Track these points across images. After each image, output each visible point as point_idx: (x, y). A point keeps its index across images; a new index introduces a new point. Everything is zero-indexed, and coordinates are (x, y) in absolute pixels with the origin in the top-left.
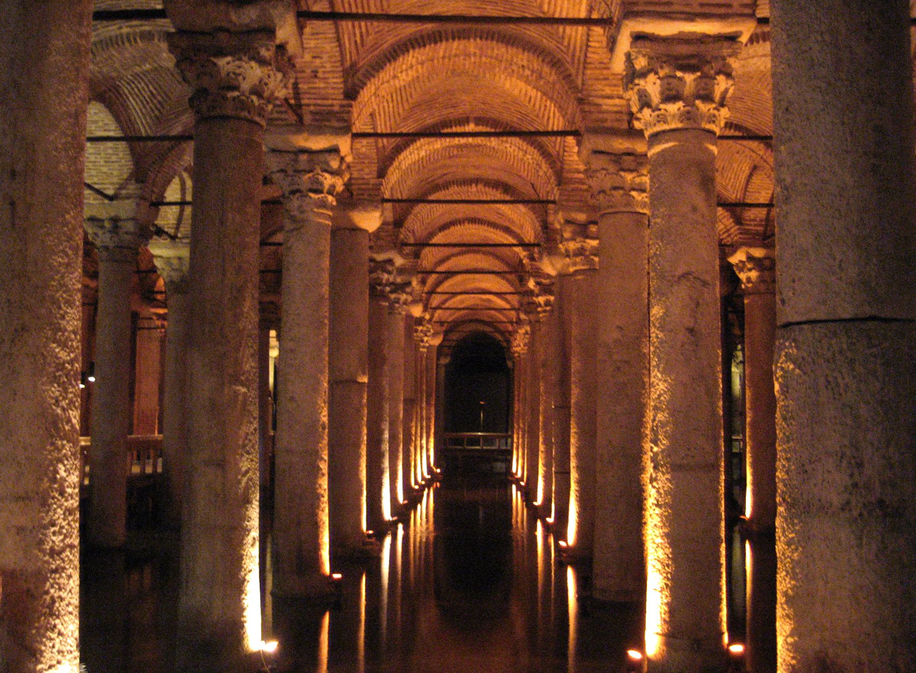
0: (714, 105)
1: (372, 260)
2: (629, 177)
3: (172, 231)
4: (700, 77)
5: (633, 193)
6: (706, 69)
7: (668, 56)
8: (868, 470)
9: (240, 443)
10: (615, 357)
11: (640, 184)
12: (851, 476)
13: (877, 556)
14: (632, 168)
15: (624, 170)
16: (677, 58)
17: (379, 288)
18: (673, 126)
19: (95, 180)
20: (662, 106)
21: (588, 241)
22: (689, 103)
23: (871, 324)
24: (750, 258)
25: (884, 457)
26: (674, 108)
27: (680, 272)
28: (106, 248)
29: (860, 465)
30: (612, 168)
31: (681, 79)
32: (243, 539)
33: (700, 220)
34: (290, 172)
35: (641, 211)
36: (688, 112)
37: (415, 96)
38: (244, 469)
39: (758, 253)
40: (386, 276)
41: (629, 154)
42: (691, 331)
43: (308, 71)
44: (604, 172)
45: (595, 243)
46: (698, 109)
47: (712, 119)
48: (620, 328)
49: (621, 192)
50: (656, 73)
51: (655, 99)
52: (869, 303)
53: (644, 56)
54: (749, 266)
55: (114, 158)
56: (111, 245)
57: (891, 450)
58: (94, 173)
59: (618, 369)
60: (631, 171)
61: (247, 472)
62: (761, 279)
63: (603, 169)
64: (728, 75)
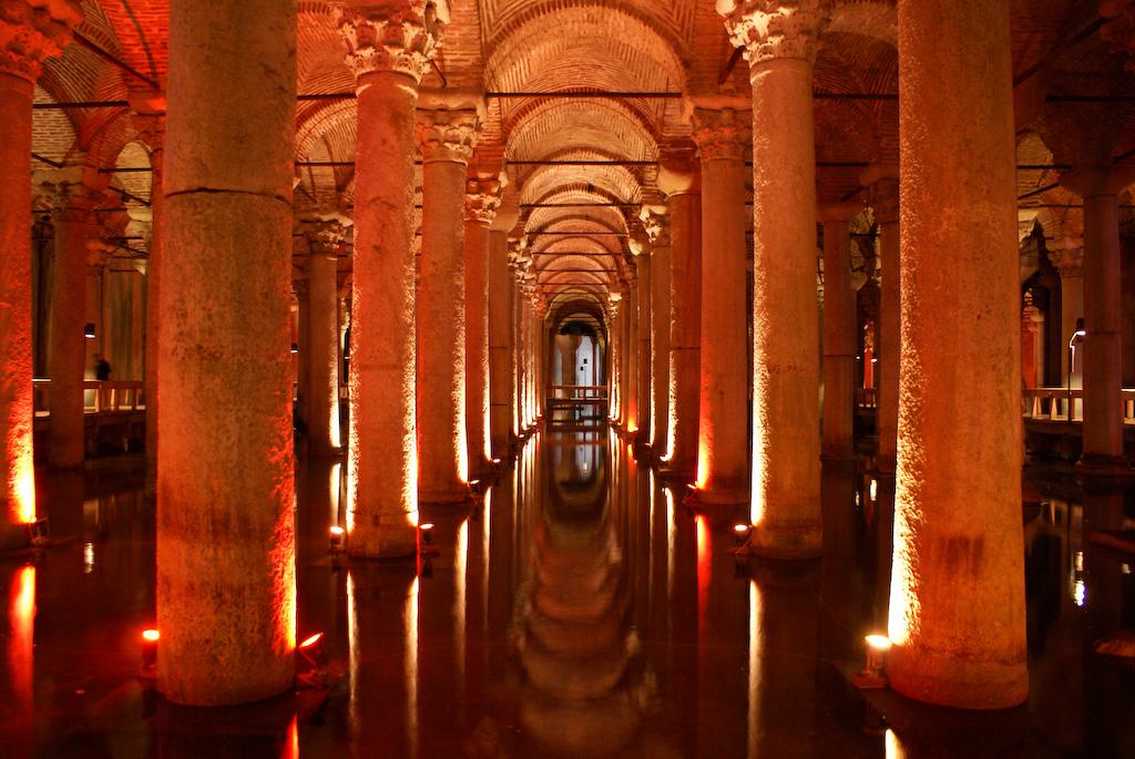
0: (402, 50)
1: (319, 221)
2: (443, 130)
3: (147, 199)
4: (389, 25)
5: (447, 145)
6: (393, 18)
7: (361, 7)
8: (191, 321)
9: (4, 350)
10: (430, 289)
11: (454, 136)
12: (179, 325)
13: (195, 393)
14: (445, 122)
16: (369, 9)
17: (326, 245)
18: (368, 70)
19: (45, 149)
20: (358, 53)
22: (378, 48)
23: (198, 195)
24: (653, 215)
25: (204, 309)
26: (368, 53)
27: (371, 196)
28: (59, 209)
29: (185, 315)
30: (428, 123)
31: (372, 27)
32: (7, 430)
33: (389, 151)
34: (153, 132)
36: (380, 57)
37: (308, 70)
38: (8, 372)
39: (660, 210)
40: (332, 235)
43: (158, 42)
46: (388, 53)
47: (405, 63)
48: (434, 263)
49: (436, 144)
50: (351, 23)
51: (355, 46)
52: (199, 177)
53: (339, 8)
54: (652, 222)
55: (58, 130)
56: (63, 206)
57: (210, 301)
58: (43, 143)
59: (432, 299)
60: (444, 125)
61: (12, 374)
62: (664, 235)
64: (414, 23)
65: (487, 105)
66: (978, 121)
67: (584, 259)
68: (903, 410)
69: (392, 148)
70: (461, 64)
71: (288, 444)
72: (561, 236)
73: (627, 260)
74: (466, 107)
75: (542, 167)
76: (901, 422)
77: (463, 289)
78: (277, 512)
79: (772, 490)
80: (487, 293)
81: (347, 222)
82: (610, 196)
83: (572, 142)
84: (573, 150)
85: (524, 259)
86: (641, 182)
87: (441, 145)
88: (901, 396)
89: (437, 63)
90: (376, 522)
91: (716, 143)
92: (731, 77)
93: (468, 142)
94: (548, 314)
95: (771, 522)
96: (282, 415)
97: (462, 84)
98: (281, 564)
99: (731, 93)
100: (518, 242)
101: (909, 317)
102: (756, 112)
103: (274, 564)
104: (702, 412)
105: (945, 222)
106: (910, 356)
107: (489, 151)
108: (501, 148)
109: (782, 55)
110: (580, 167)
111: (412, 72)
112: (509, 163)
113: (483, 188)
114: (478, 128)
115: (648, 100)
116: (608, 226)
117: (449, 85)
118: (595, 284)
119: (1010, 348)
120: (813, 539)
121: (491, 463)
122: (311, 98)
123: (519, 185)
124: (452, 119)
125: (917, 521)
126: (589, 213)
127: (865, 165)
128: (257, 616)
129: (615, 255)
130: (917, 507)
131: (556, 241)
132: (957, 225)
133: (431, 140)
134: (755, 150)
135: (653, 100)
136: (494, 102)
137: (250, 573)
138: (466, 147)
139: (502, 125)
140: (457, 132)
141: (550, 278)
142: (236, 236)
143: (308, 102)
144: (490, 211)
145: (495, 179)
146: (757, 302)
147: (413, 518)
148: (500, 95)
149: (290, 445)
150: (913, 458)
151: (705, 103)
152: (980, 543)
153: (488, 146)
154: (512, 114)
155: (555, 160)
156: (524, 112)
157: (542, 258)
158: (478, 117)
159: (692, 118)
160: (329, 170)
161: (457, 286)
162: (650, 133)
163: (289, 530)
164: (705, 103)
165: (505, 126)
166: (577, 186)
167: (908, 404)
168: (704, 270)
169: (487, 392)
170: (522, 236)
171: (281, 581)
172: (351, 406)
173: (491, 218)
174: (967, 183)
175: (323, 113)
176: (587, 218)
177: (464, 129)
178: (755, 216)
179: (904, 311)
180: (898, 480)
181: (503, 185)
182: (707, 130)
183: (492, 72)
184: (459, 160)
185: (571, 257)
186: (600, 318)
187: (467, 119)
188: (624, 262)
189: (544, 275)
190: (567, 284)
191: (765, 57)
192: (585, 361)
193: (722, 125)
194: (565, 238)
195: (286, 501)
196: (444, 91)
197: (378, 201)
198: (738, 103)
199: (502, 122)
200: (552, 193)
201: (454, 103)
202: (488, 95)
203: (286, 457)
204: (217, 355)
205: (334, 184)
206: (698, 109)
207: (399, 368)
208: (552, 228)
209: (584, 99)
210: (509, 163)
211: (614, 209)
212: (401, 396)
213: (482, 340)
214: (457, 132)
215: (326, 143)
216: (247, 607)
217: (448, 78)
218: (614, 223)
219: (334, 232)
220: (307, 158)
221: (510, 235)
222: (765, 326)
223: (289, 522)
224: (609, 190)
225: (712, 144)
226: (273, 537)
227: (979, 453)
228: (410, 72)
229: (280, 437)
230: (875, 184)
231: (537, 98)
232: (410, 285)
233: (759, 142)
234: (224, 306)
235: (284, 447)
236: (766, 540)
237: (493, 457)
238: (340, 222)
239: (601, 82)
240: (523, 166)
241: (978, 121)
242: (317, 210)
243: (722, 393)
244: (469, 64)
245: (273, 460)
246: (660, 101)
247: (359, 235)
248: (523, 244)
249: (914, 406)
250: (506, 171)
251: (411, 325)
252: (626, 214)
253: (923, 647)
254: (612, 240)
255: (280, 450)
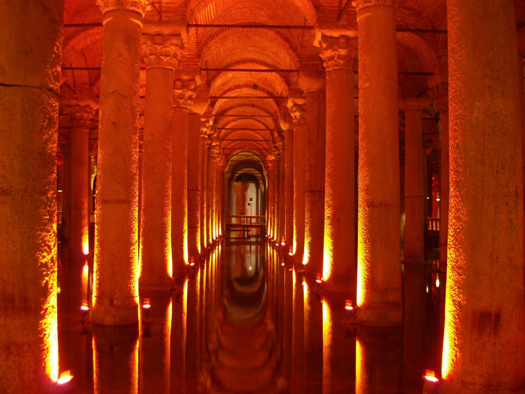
1: (78, 105)
2: (159, 48)
5: (162, 57)
11: (166, 52)
15: (155, 44)
18: (111, 9)
21: (175, 90)
24: (295, 105)
35: (167, 67)
39: (300, 102)
40: (86, 115)
41: (159, 35)
42: (114, 124)
44: (145, 46)
45: (179, 92)
48: (153, 134)
49: (155, 56)
54: (294, 109)
60: (160, 44)
62: (302, 117)
63: (144, 43)
65: (188, 32)
66: (495, 49)
67: (251, 132)
68: (451, 232)
69: (125, 59)
70: (171, 5)
71: (53, 251)
72: (236, 118)
73: (278, 134)
74: (176, 33)
75: (224, 72)
76: (450, 239)
77: (171, 152)
78: (45, 292)
79: (370, 284)
80: (186, 154)
81: (95, 107)
82: (267, 92)
83: (244, 57)
84: (245, 61)
85: (212, 132)
86: (288, 83)
87: (158, 57)
88: (450, 222)
89: (156, 5)
90: (111, 303)
91: (336, 59)
92: (345, 17)
93: (175, 56)
94: (227, 168)
95: (369, 304)
96: (50, 232)
97: (172, 18)
98: (47, 329)
99: (345, 27)
100: (208, 121)
101: (455, 171)
102: (360, 40)
103: (44, 329)
104: (325, 233)
105: (476, 112)
106: (455, 196)
107: (189, 62)
108: (197, 60)
109: (377, 4)
110: (249, 73)
111: (140, 11)
112: (202, 69)
113: (184, 86)
114: (182, 47)
115: (292, 30)
116: (267, 111)
117: (164, 19)
118: (258, 149)
119: (516, 192)
120: (395, 316)
121: (189, 266)
122: (75, 25)
123: (208, 84)
124: (166, 40)
125: (460, 302)
126: (254, 103)
127: (432, 74)
128: (32, 363)
129: (271, 131)
130: (459, 293)
131: (233, 121)
132: (483, 113)
133: (151, 54)
134: (360, 64)
135: (295, 30)
136: (193, 30)
137: (28, 335)
138: (174, 59)
139: (197, 45)
140: (168, 49)
141: (229, 144)
142: (23, 115)
143: (72, 28)
144: (189, 101)
145: (193, 80)
146: (361, 162)
147: (137, 300)
148: (197, 26)
149: (54, 251)
150: (457, 261)
151: (328, 33)
152: (498, 316)
153: (189, 58)
154: (205, 38)
155: (232, 68)
156: (212, 37)
157: (224, 131)
158: (182, 40)
159: (320, 42)
160: (86, 72)
161: (167, 149)
162: (294, 51)
163: (53, 307)
164: (328, 33)
165: (200, 45)
166: (246, 86)
167: (454, 227)
168: (327, 140)
169: (186, 219)
170: (211, 117)
171: (47, 340)
172: (96, 227)
173: (190, 105)
174: (489, 87)
175: (82, 35)
176: (253, 106)
177: (173, 48)
178: (359, 106)
179: (451, 168)
180: (448, 276)
181: (198, 84)
182: (330, 50)
183: (192, 11)
184: (170, 68)
185: (243, 132)
186: (261, 172)
187: (175, 41)
188: (276, 135)
189: (225, 143)
190: (239, 149)
191: (366, 5)
192: (251, 200)
193: (341, 48)
194: (238, 119)
195: (51, 288)
196: (160, 22)
197: (116, 93)
198: (350, 33)
199: (198, 43)
200: (230, 89)
201: (166, 30)
202: (189, 26)
203: (52, 258)
204: (8, 192)
205: (88, 82)
206: (324, 36)
207: (128, 202)
208: (230, 113)
209: (251, 29)
210: (202, 69)
211: (270, 100)
212: (129, 221)
213: (183, 185)
214: (168, 49)
215: (84, 55)
216: (26, 357)
217: (163, 15)
218: (270, 110)
219: (88, 113)
220: (71, 65)
221: (203, 116)
222: (365, 177)
223: (53, 301)
224: (267, 88)
225: (334, 60)
226: (43, 312)
227: (498, 258)
228: (138, 10)
229: (49, 247)
230: (438, 86)
231: (221, 28)
232: (135, 148)
233: (363, 60)
234: (13, 160)
235: (51, 252)
236: (363, 316)
237: (190, 261)
238: (92, 106)
239: (262, 18)
240: (211, 72)
241: (495, 49)
242: (77, 98)
243: (338, 220)
244: (177, 5)
245: (44, 261)
246: (300, 31)
247: (103, 115)
248: (211, 123)
249: (457, 229)
250: (200, 75)
251: (136, 174)
252: (278, 104)
253: (462, 382)
254: (269, 121)
255: (48, 255)
